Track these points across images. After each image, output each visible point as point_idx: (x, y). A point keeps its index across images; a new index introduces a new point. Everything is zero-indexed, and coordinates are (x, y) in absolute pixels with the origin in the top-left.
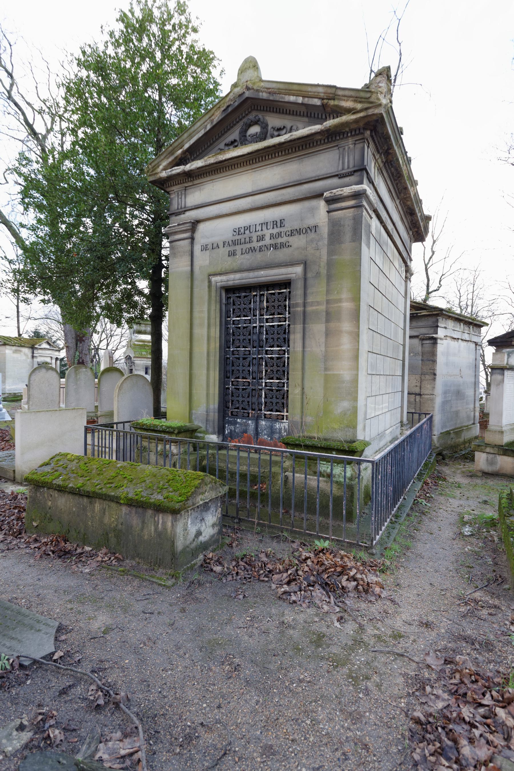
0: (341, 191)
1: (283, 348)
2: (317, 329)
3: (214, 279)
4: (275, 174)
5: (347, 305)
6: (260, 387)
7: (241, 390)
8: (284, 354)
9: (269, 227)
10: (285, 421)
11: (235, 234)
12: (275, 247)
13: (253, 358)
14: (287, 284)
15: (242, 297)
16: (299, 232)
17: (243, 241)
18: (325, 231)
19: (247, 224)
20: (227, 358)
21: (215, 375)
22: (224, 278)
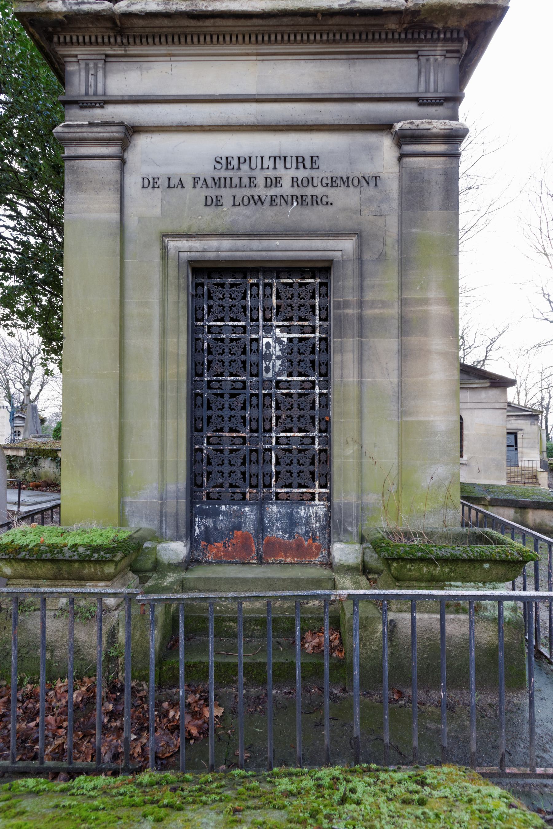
0: (429, 123)
1: (310, 378)
2: (385, 346)
3: (173, 244)
4: (302, 74)
5: (436, 310)
6: (267, 447)
7: (226, 453)
8: (313, 388)
9: (288, 166)
10: (317, 502)
11: (218, 166)
12: (302, 201)
13: (252, 395)
14: (323, 269)
15: (227, 286)
16: (347, 182)
17: (236, 181)
18: (393, 187)
19: (244, 152)
20: (197, 394)
21: (178, 426)
22: (197, 244)
